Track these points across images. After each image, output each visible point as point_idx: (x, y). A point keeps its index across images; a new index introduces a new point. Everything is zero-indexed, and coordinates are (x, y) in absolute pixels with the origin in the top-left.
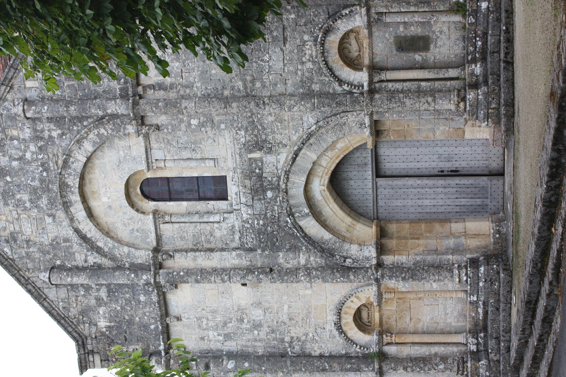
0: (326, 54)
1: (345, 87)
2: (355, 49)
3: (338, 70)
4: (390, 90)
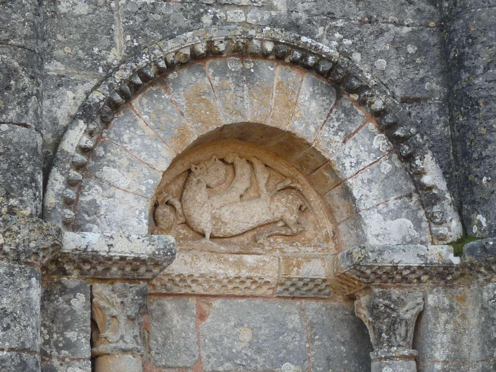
0: (234, 65)
2: (226, 214)
3: (159, 113)
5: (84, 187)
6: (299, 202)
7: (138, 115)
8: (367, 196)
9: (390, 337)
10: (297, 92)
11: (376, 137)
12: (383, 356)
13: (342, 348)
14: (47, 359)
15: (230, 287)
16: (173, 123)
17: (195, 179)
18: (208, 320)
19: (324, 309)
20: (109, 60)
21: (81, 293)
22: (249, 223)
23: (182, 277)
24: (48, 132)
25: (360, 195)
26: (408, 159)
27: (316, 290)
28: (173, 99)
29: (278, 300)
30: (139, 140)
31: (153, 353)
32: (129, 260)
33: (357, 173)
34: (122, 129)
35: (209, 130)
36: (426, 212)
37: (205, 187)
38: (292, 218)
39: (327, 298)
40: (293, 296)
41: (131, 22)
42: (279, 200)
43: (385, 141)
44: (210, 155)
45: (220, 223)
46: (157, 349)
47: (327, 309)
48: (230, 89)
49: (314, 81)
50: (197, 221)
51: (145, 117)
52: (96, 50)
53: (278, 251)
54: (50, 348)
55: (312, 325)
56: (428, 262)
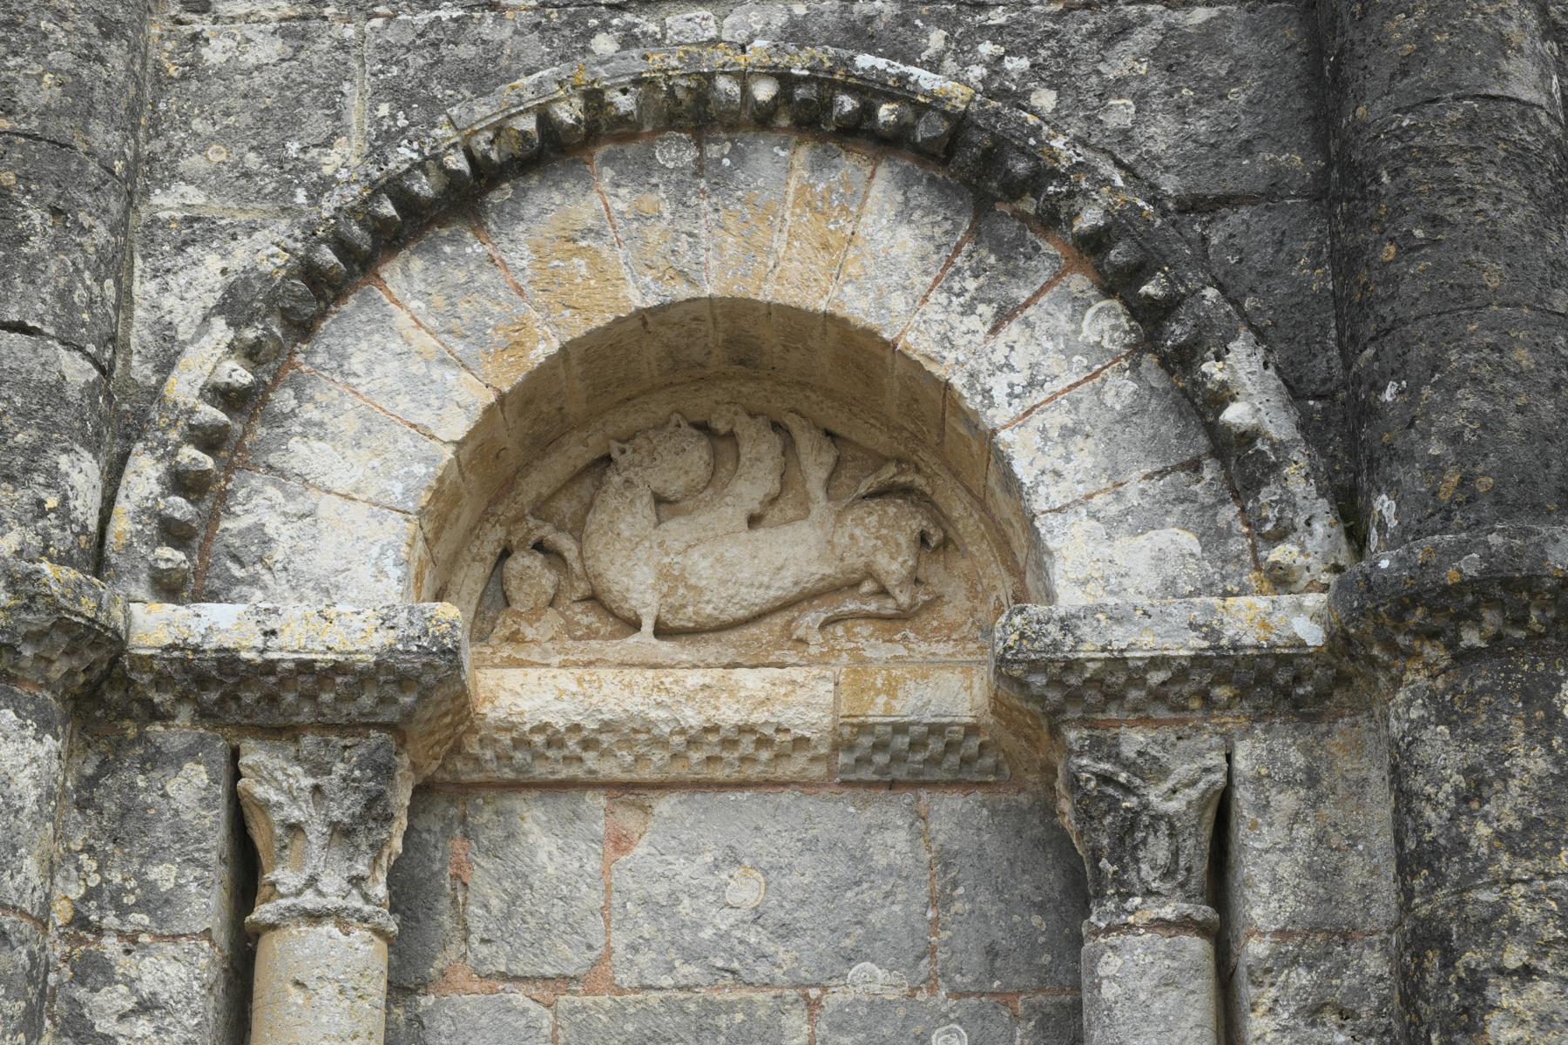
0: (675, 154)
1: (210, 359)
2: (701, 566)
4: (93, 971)
5: (233, 492)
6: (917, 523)
7: (396, 302)
8: (1057, 474)
9: (1124, 869)
10: (853, 209)
11: (1091, 312)
12: (1102, 925)
13: (1036, 920)
14: (90, 937)
15: (696, 756)
16: (491, 316)
17: (616, 480)
18: (640, 850)
19: (985, 812)
20: (328, 171)
21: (199, 763)
22: (768, 587)
23: (549, 732)
24: (146, 360)
25: (1036, 472)
26: (1181, 361)
27: (953, 759)
28: (496, 255)
29: (847, 791)
30: (393, 366)
31: (474, 940)
32: (322, 669)
33: (1027, 413)
34: (348, 340)
35: (593, 326)
36: (1243, 510)
37: (646, 499)
38: (895, 566)
39: (995, 783)
40: (888, 778)
41: (395, 70)
42: (859, 522)
43: (1123, 319)
44: (663, 412)
45: (681, 591)
46: (487, 929)
47: (993, 813)
48: (660, 217)
49: (906, 170)
50: (617, 587)
51: (414, 304)
52: (293, 147)
53: (845, 657)
54: (100, 908)
55: (945, 860)
56: (1224, 642)
